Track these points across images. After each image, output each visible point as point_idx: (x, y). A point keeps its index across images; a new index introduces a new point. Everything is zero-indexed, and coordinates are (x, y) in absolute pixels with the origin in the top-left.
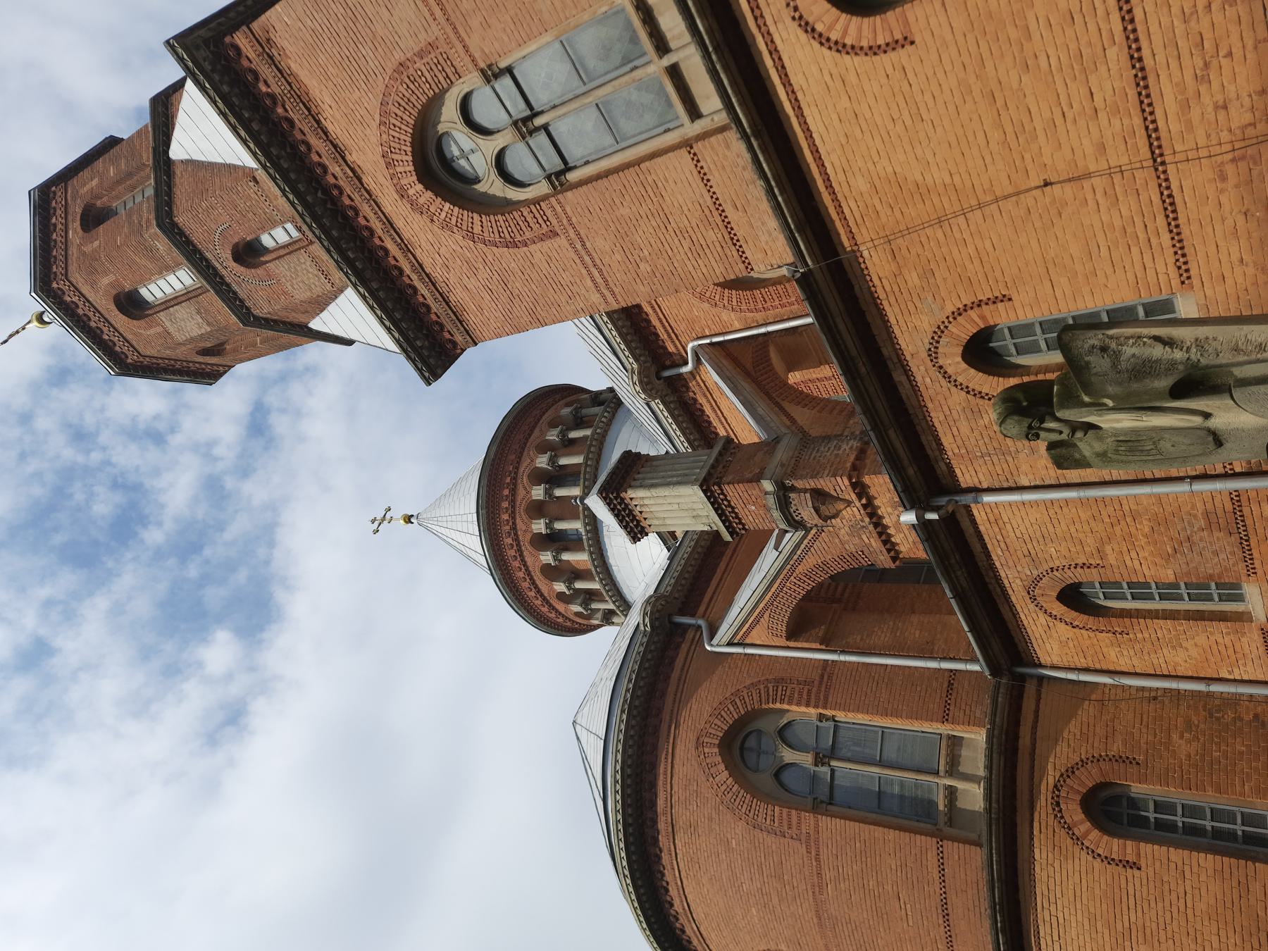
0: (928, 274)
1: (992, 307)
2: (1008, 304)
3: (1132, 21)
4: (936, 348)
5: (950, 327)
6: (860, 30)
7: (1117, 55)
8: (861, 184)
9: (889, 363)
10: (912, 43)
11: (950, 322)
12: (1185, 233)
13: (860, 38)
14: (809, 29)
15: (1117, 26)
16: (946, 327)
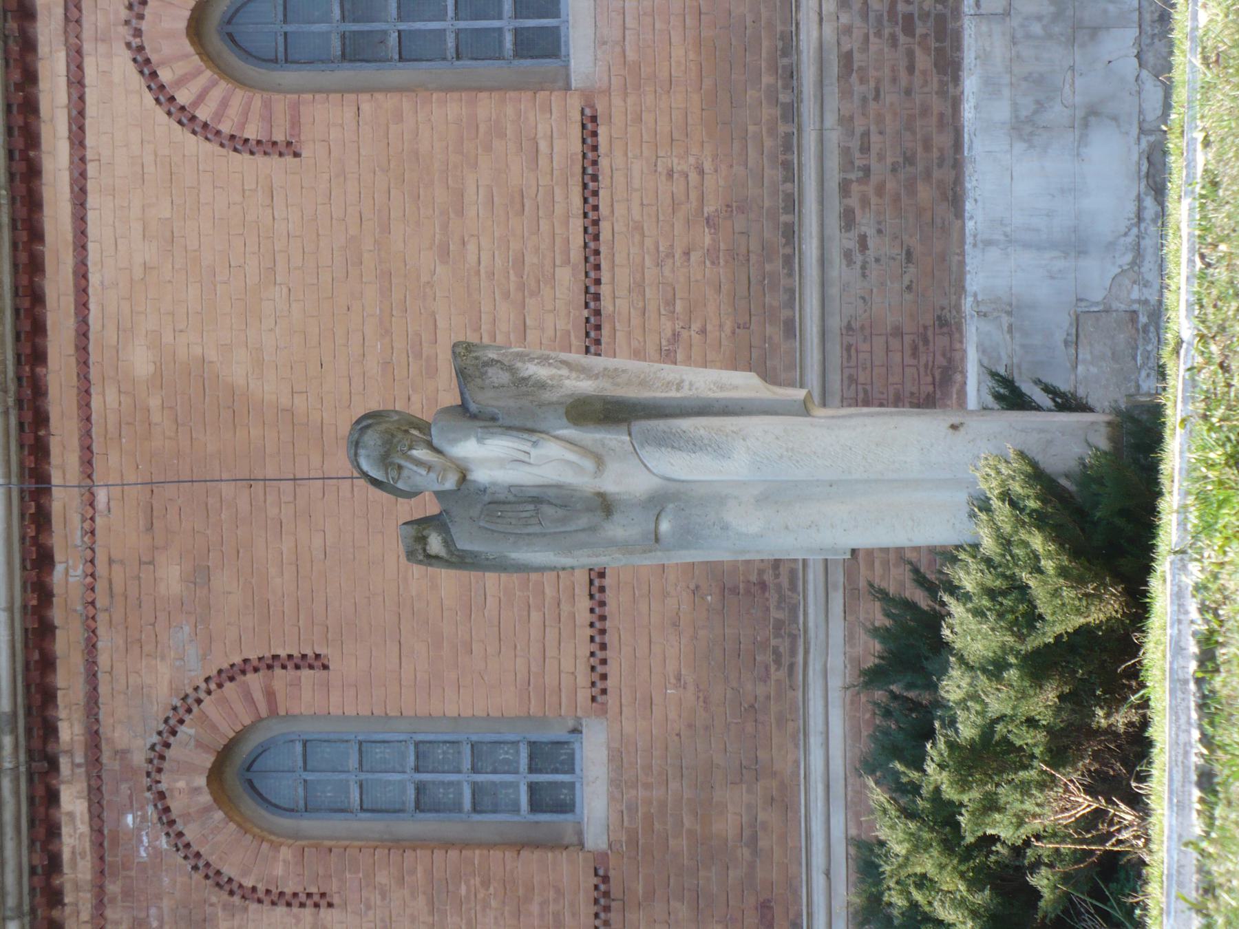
0: (200, 575)
1: (291, 673)
2: (318, 674)
3: (596, 238)
4: (167, 745)
5: (207, 700)
6: (224, 103)
7: (568, 281)
8: (141, 362)
9: (64, 764)
10: (296, 155)
11: (209, 692)
12: (609, 596)
13: (219, 114)
14: (146, 71)
15: (577, 239)
16: (199, 701)
